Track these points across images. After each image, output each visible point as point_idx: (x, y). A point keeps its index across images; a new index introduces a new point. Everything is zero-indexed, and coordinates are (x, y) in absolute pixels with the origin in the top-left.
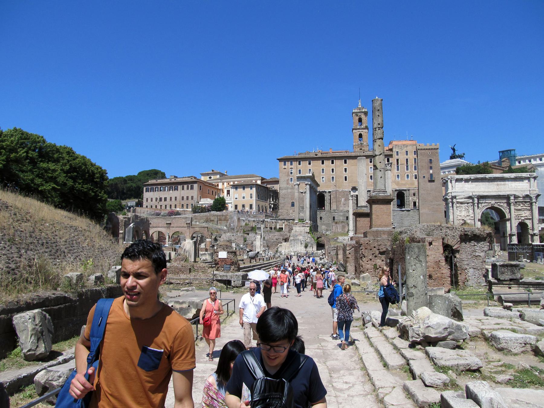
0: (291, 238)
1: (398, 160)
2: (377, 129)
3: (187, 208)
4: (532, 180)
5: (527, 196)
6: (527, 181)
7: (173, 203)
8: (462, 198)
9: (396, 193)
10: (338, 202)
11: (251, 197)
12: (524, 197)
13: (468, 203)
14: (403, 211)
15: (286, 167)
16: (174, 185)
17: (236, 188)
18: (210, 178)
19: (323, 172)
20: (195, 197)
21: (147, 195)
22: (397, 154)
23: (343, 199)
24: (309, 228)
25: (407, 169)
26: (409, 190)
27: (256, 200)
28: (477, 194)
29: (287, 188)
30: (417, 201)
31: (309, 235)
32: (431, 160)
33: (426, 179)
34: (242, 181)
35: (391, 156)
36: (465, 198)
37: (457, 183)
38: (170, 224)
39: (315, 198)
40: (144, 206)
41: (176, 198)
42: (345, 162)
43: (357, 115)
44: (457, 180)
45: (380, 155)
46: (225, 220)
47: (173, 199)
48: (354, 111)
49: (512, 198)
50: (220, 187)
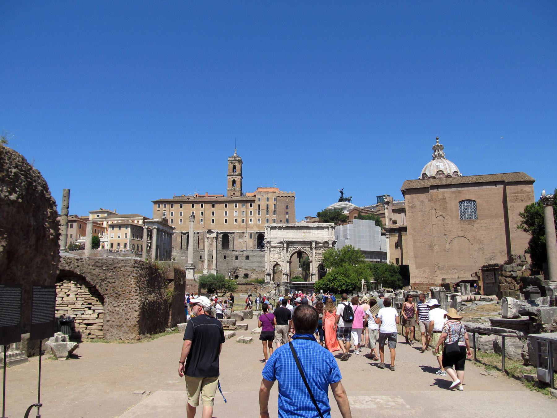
1: (259, 206)
4: (330, 229)
5: (326, 242)
6: (327, 230)
9: (257, 235)
11: (126, 237)
12: (323, 243)
13: (280, 248)
14: (262, 251)
15: (160, 209)
17: (113, 228)
18: (98, 216)
20: (74, 235)
22: (259, 200)
25: (267, 214)
27: (131, 240)
28: (287, 240)
32: (287, 206)
35: (254, 201)
42: (213, 206)
43: (232, 163)
44: (272, 228)
49: (314, 244)
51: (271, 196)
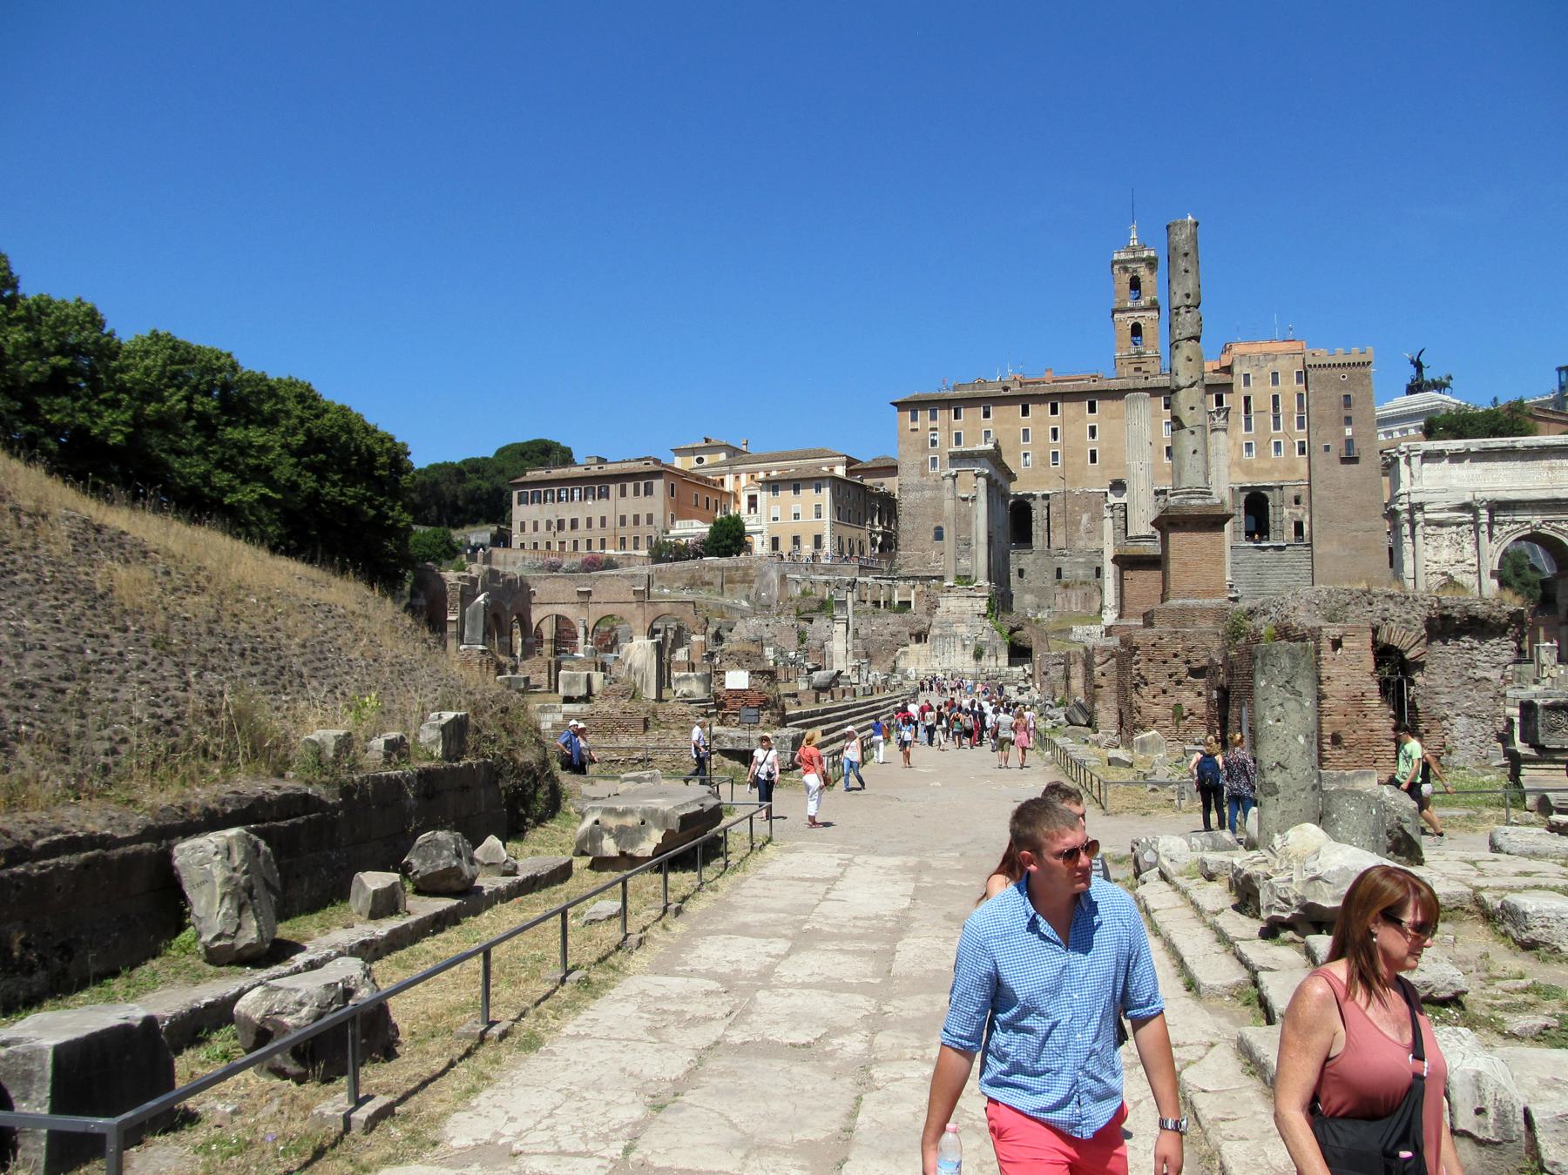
0: (935, 631)
1: (1247, 399)
2: (1182, 310)
3: (636, 548)
7: (597, 533)
8: (1441, 510)
9: (1243, 496)
10: (1071, 524)
11: (819, 515)
13: (1459, 525)
14: (1264, 549)
15: (917, 425)
16: (597, 484)
17: (775, 490)
18: (700, 460)
19: (1026, 438)
20: (658, 517)
21: (521, 513)
22: (1247, 383)
23: (1085, 518)
24: (984, 602)
25: (1277, 427)
26: (1281, 488)
27: (833, 524)
28: (1489, 496)
29: (922, 488)
30: (1307, 518)
31: (987, 623)
32: (1347, 397)
33: (1334, 455)
34: (792, 467)
35: (1228, 387)
36: (1450, 510)
37: (1426, 465)
38: (589, 593)
39: (1004, 514)
40: (516, 544)
41: (603, 519)
42: (1092, 409)
43: (1126, 270)
44: (1427, 457)
45: (1191, 386)
46: (743, 582)
47: (596, 523)
48: (1116, 257)
50: (729, 485)
51: (1288, 368)
